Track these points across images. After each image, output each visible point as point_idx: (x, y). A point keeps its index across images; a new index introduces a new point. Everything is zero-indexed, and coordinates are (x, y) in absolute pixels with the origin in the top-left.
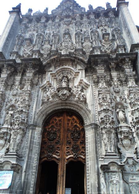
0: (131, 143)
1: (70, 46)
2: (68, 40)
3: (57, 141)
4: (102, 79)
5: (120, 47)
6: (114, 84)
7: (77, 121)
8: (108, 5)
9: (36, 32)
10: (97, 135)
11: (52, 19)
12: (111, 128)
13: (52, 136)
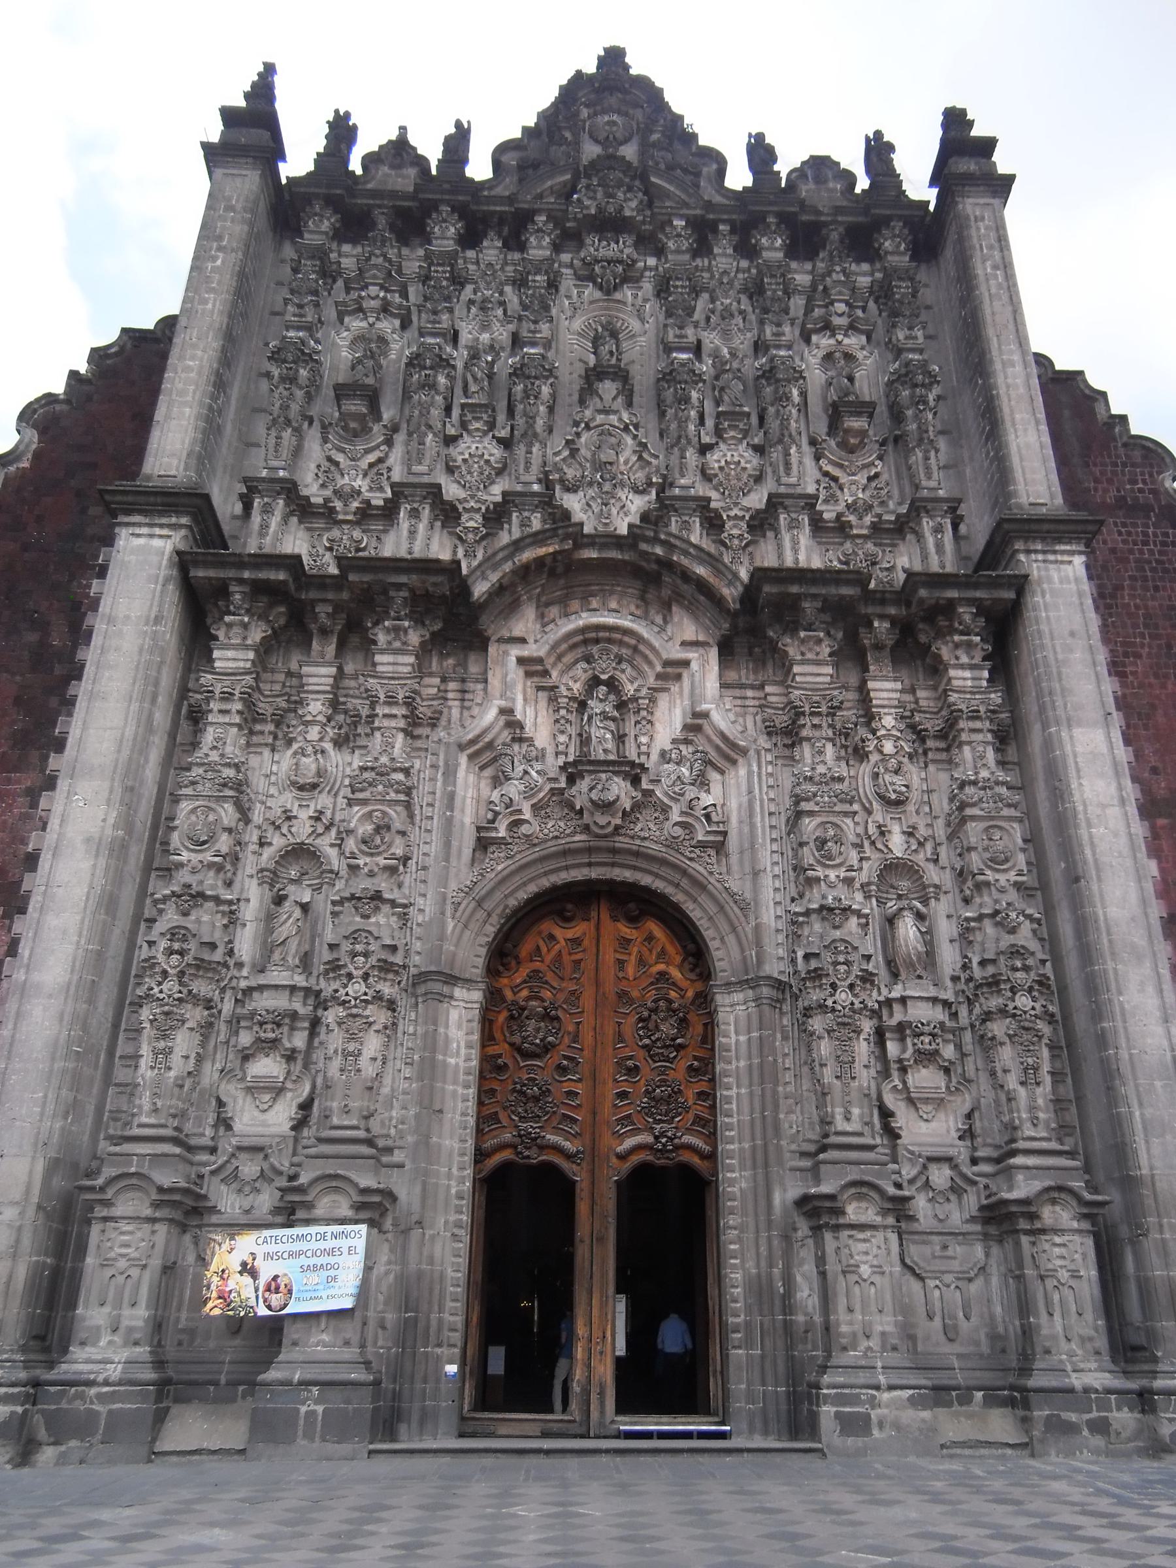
0: (948, 1088)
1: (626, 462)
2: (613, 419)
3: (566, 1057)
4: (816, 721)
5: (927, 512)
6: (881, 752)
7: (670, 949)
9: (397, 323)
10: (779, 1036)
11: (506, 230)
12: (854, 1012)
13: (538, 1030)
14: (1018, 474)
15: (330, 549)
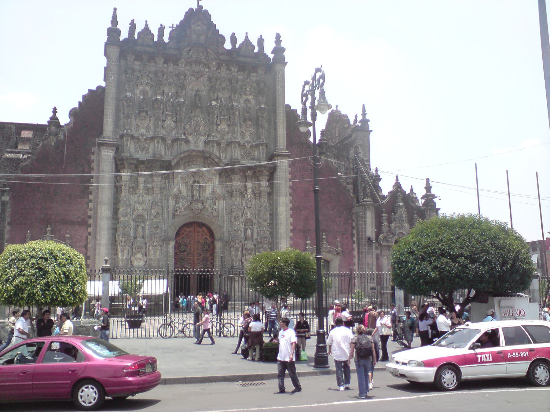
3: (188, 252)
4: (236, 193)
8: (261, 41)
14: (279, 141)
15: (139, 147)
